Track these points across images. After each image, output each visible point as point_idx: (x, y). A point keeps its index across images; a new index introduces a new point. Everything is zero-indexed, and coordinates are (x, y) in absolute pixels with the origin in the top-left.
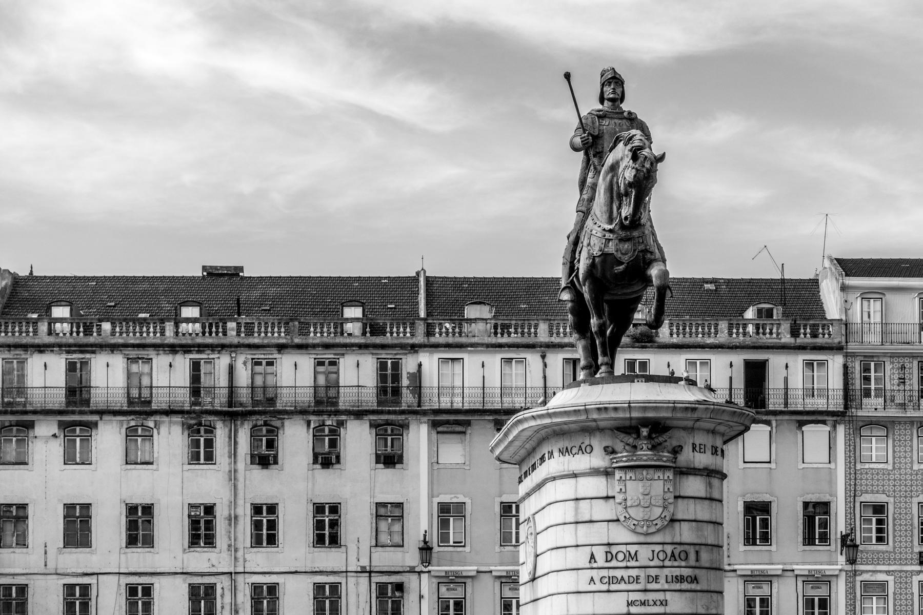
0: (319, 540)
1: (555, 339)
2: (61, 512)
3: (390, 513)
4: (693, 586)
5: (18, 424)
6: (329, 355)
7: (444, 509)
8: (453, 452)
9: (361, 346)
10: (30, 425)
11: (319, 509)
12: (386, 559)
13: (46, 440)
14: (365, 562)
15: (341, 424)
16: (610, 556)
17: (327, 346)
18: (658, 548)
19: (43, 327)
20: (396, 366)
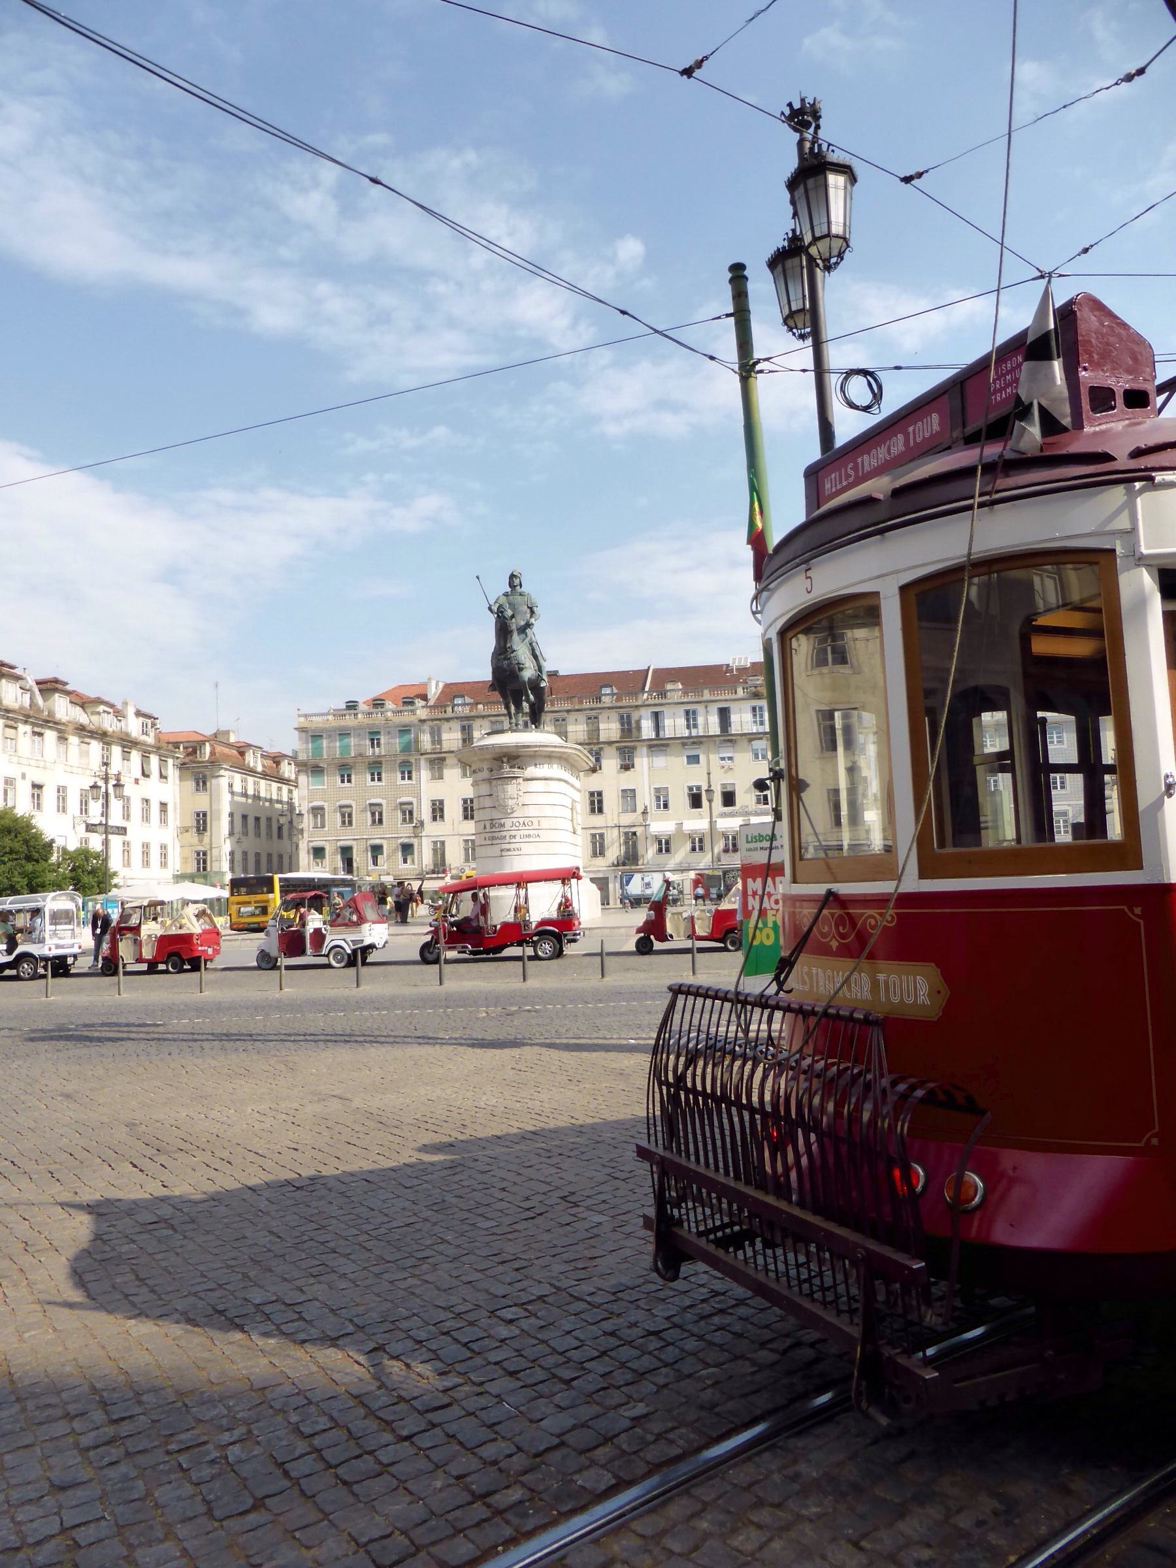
0: (593, 811)
1: (713, 698)
2: (461, 802)
3: (629, 795)
4: (537, 839)
5: (438, 759)
6: (593, 713)
7: (657, 790)
8: (660, 761)
9: (609, 708)
10: (444, 759)
11: (592, 794)
12: (628, 819)
13: (452, 767)
14: (616, 822)
15: (601, 749)
16: (492, 826)
17: (592, 709)
18: (515, 820)
19: (449, 709)
20: (629, 717)
